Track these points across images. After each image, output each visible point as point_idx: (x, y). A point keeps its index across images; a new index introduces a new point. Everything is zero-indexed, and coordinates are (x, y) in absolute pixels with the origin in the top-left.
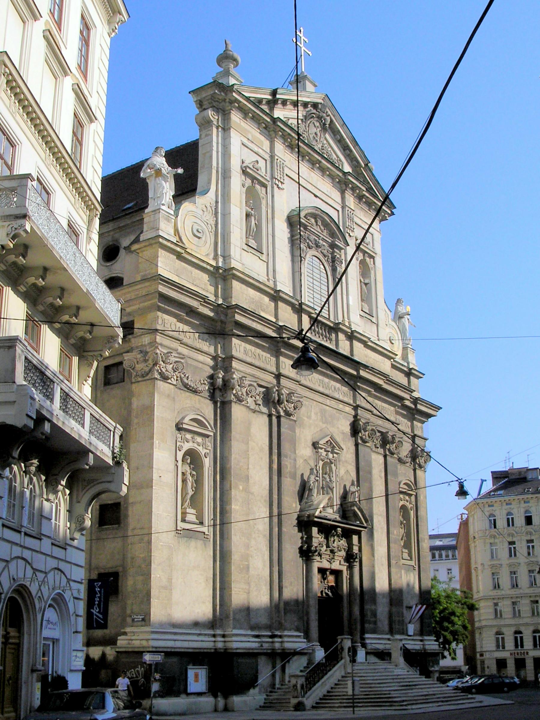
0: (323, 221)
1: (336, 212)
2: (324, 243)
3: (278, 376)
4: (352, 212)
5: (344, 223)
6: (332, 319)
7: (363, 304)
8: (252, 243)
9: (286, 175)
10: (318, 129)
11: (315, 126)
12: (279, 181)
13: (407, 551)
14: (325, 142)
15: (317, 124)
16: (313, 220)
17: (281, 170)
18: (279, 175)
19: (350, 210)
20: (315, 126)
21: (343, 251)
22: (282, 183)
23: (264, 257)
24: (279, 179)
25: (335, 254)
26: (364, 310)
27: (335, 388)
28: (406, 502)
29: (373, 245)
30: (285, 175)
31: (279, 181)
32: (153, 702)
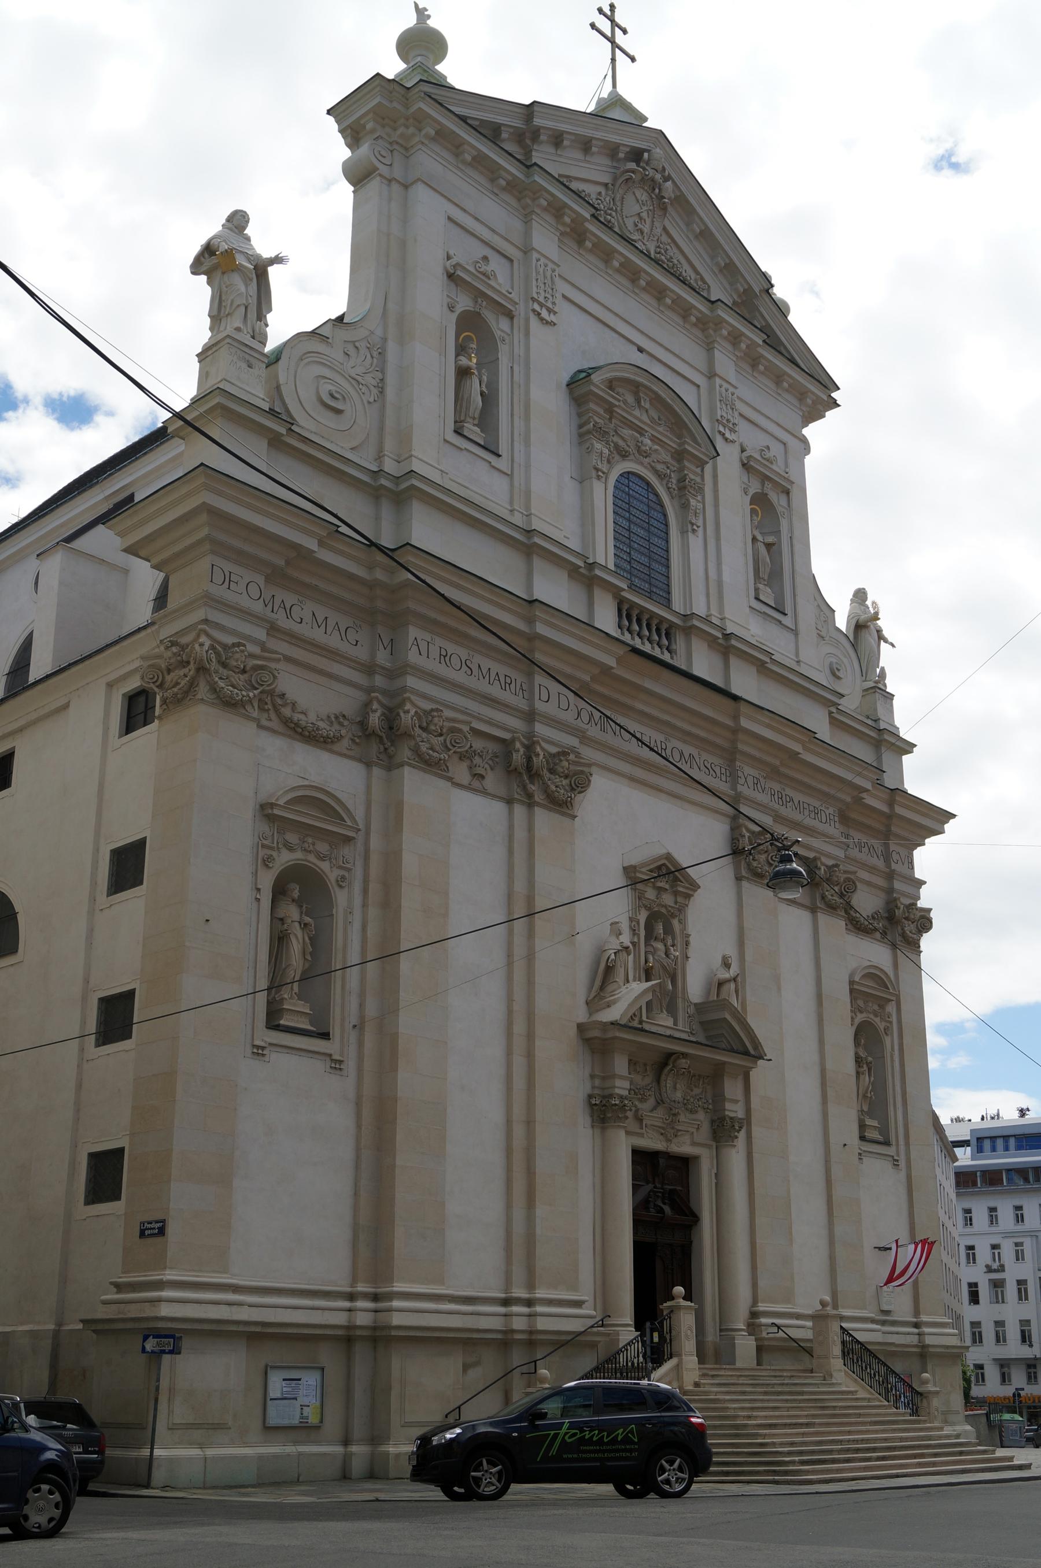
0: (657, 400)
1: (694, 389)
2: (656, 447)
3: (530, 716)
4: (731, 389)
5: (712, 410)
6: (677, 604)
7: (761, 586)
8: (471, 429)
9: (564, 296)
10: (645, 208)
11: (638, 201)
12: (541, 305)
13: (875, 1123)
14: (664, 238)
15: (644, 197)
16: (630, 399)
17: (549, 282)
18: (543, 293)
19: (725, 385)
20: (638, 201)
21: (708, 468)
22: (550, 311)
23: (502, 464)
24: (541, 299)
25: (686, 472)
26: (762, 598)
27: (682, 754)
28: (872, 1016)
29: (787, 465)
30: (559, 296)
31: (541, 305)
32: (157, 1452)
